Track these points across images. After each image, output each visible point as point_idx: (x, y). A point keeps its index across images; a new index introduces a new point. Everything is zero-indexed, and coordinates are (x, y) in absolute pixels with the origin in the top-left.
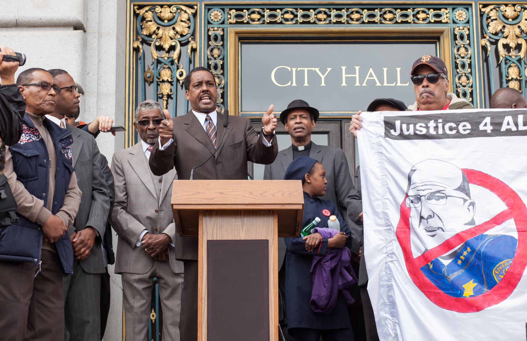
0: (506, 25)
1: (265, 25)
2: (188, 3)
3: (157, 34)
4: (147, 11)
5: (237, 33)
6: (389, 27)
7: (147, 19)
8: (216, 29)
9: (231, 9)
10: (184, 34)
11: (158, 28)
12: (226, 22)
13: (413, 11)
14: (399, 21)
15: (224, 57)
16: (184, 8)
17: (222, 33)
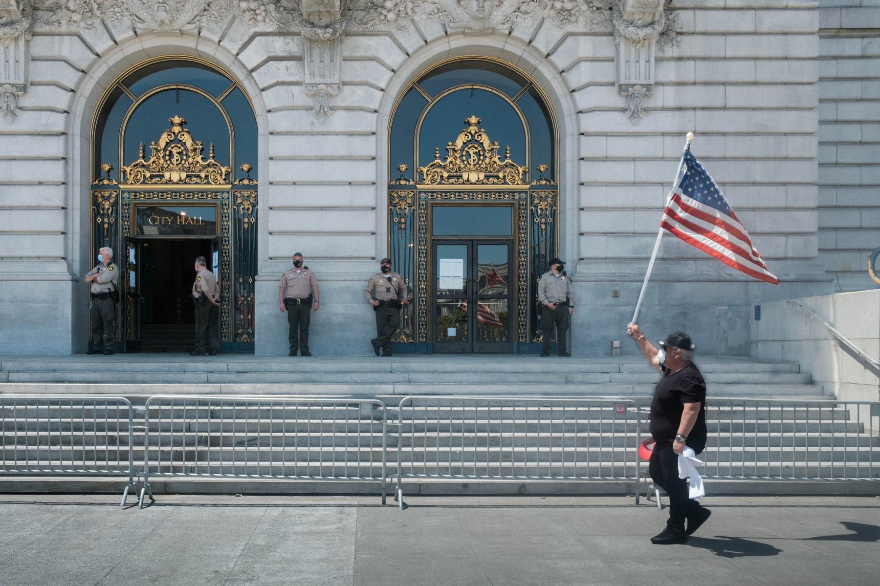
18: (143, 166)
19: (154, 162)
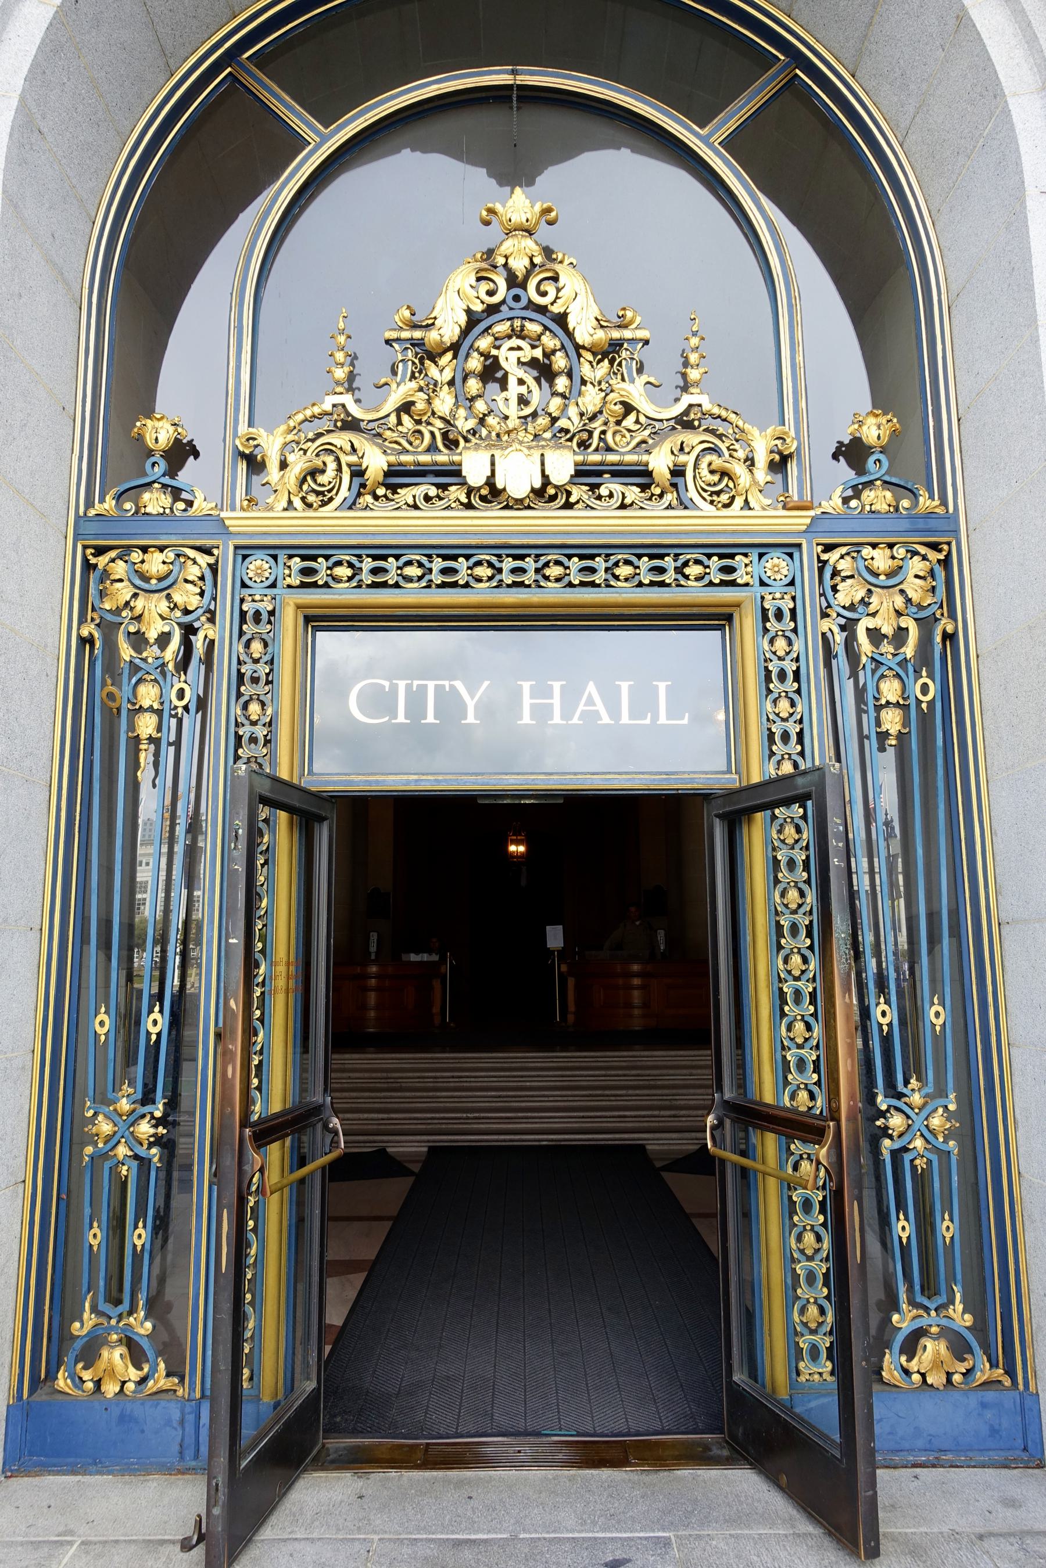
0: (873, 588)
1: (363, 590)
2: (198, 543)
3: (132, 609)
4: (113, 561)
5: (298, 607)
6: (624, 594)
7: (112, 577)
8: (258, 597)
9: (291, 557)
10: (190, 608)
11: (135, 596)
12: (279, 584)
13: (675, 561)
14: (647, 582)
15: (272, 659)
16: (191, 553)
17: (270, 608)
18: (351, 425)
19: (406, 407)
